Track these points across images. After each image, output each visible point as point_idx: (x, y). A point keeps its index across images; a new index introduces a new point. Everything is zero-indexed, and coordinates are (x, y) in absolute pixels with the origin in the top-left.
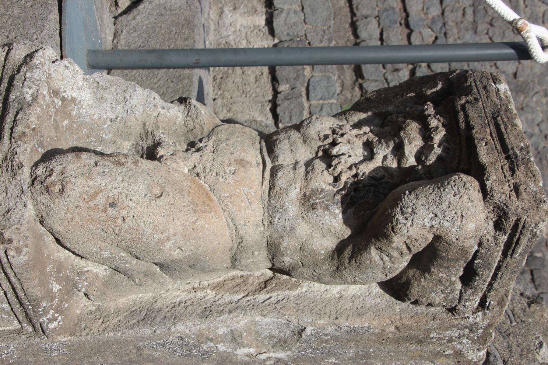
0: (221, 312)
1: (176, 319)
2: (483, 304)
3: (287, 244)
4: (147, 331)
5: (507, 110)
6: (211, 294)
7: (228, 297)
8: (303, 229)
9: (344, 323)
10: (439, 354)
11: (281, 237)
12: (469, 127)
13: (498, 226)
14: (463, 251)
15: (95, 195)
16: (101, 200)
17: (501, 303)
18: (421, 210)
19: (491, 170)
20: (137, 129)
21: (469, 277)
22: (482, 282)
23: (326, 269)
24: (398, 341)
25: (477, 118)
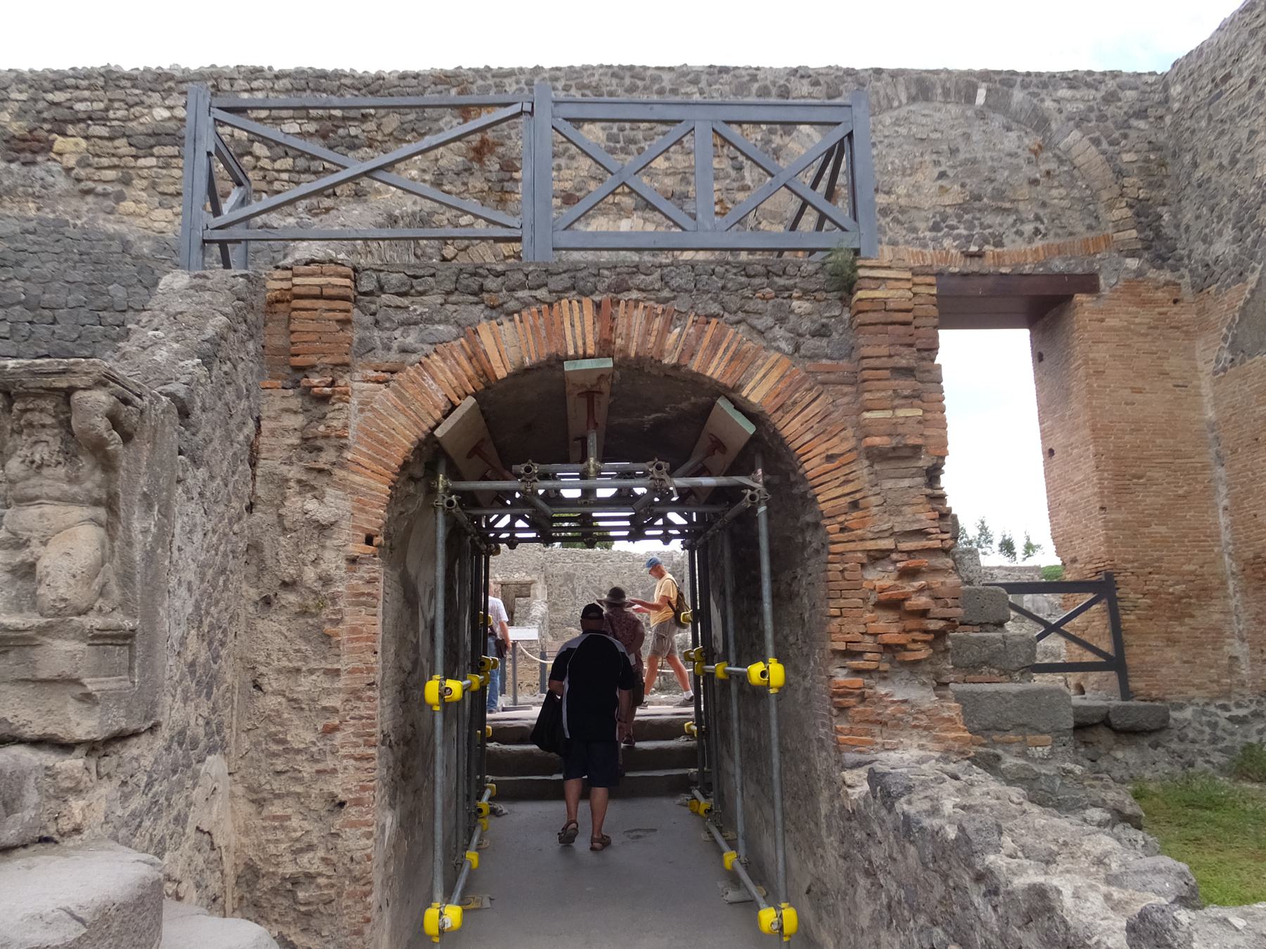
0: (130, 537)
1: (132, 560)
2: (140, 396)
3: (96, 494)
4: (138, 577)
5: (29, 365)
6: (117, 543)
7: (120, 533)
8: (88, 485)
9: (143, 470)
10: (163, 422)
11: (91, 497)
12: (41, 388)
13: (105, 385)
14: (115, 403)
15: (70, 585)
16: (72, 582)
17: (139, 386)
18: (93, 421)
19: (73, 383)
20: (7, 577)
21: (126, 402)
22: (130, 395)
23: (112, 476)
24: (155, 443)
25: (32, 383)
